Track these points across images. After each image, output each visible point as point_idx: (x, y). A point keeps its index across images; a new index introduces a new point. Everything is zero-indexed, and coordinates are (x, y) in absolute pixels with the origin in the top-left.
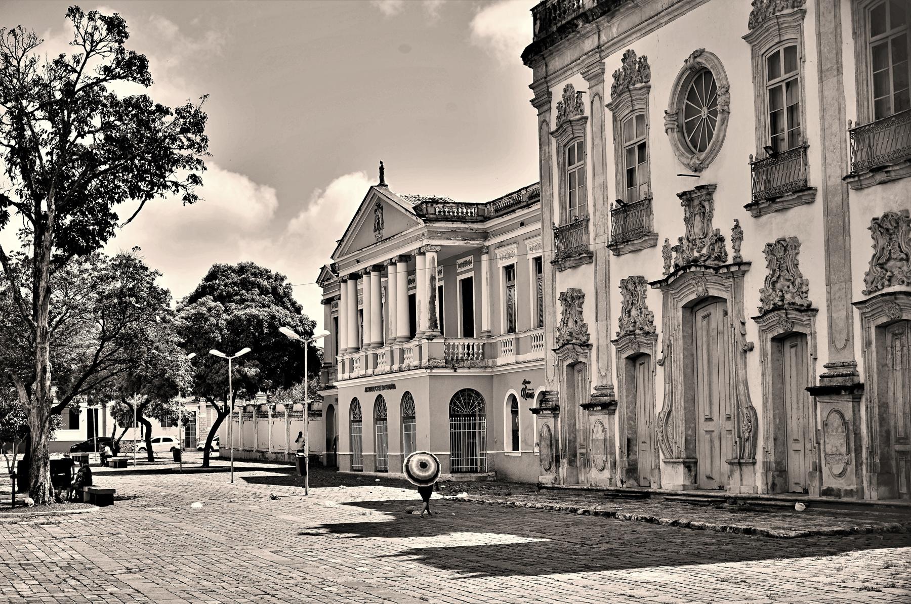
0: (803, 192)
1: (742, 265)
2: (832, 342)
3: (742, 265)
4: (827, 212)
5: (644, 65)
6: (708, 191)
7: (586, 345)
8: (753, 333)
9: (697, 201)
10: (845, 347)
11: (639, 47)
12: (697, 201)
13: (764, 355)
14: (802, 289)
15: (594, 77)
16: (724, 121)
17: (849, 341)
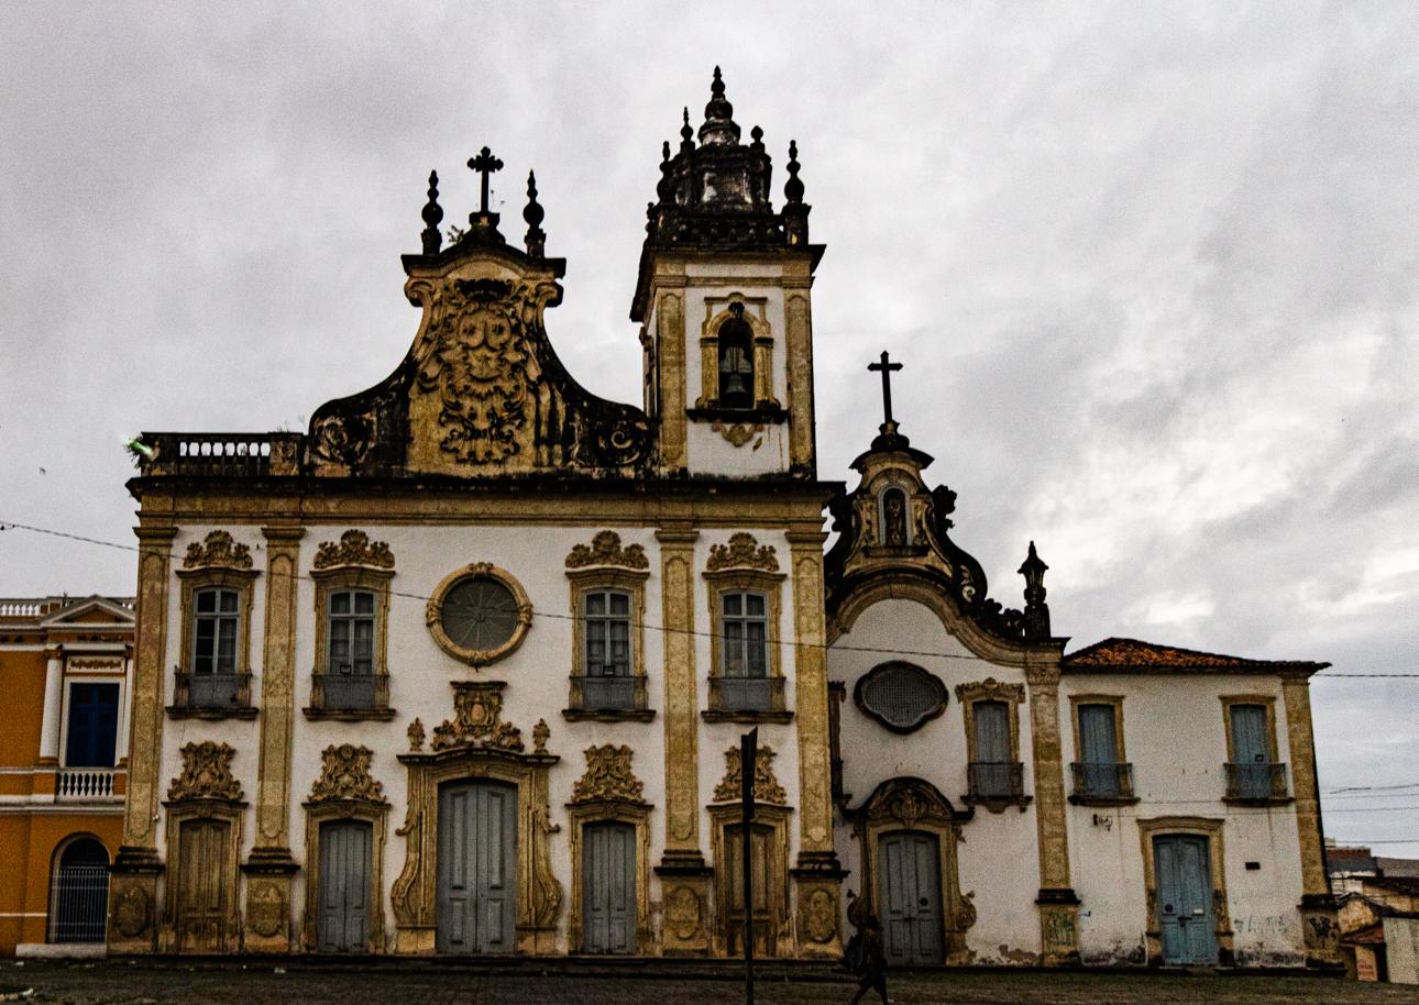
0: (646, 716)
1: (544, 763)
2: (671, 833)
3: (544, 763)
4: (668, 731)
5: (382, 553)
6: (500, 686)
7: (238, 805)
8: (560, 818)
9: (479, 696)
10: (687, 838)
11: (375, 533)
12: (479, 696)
13: (574, 834)
14: (637, 787)
15: (284, 539)
16: (525, 633)
17: (693, 834)
